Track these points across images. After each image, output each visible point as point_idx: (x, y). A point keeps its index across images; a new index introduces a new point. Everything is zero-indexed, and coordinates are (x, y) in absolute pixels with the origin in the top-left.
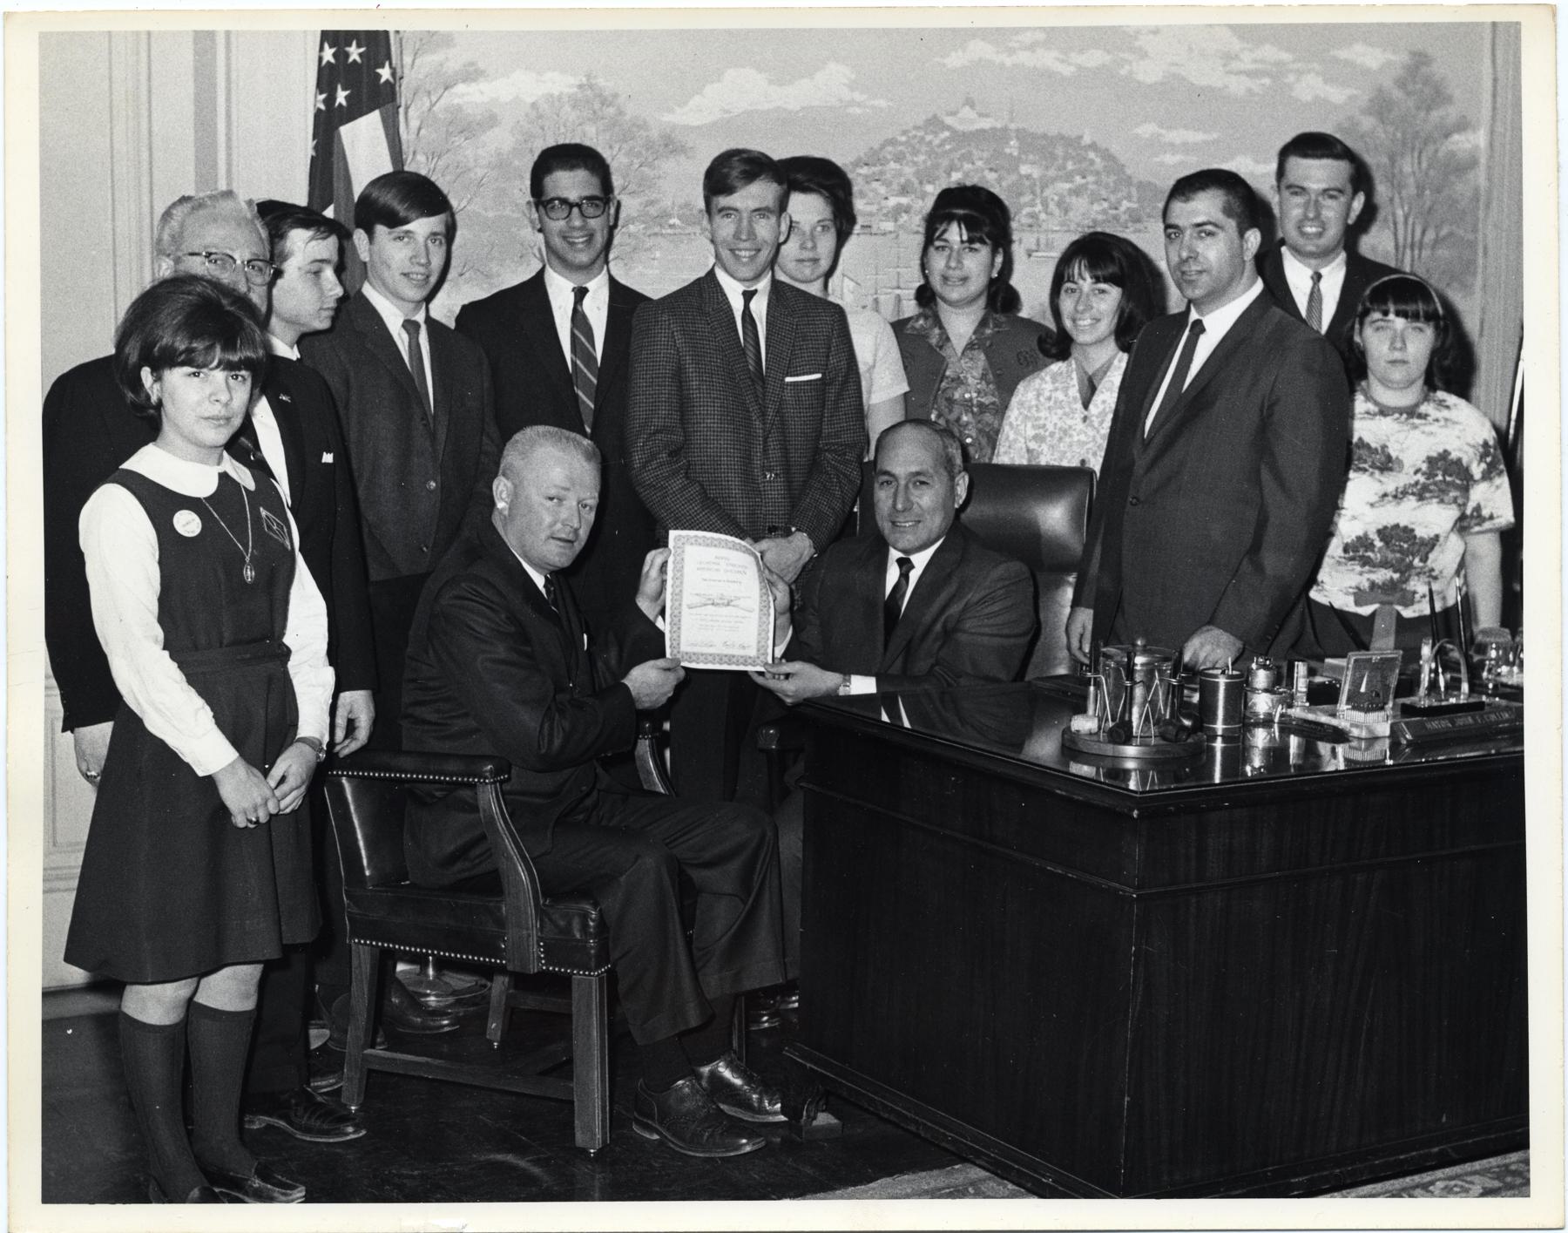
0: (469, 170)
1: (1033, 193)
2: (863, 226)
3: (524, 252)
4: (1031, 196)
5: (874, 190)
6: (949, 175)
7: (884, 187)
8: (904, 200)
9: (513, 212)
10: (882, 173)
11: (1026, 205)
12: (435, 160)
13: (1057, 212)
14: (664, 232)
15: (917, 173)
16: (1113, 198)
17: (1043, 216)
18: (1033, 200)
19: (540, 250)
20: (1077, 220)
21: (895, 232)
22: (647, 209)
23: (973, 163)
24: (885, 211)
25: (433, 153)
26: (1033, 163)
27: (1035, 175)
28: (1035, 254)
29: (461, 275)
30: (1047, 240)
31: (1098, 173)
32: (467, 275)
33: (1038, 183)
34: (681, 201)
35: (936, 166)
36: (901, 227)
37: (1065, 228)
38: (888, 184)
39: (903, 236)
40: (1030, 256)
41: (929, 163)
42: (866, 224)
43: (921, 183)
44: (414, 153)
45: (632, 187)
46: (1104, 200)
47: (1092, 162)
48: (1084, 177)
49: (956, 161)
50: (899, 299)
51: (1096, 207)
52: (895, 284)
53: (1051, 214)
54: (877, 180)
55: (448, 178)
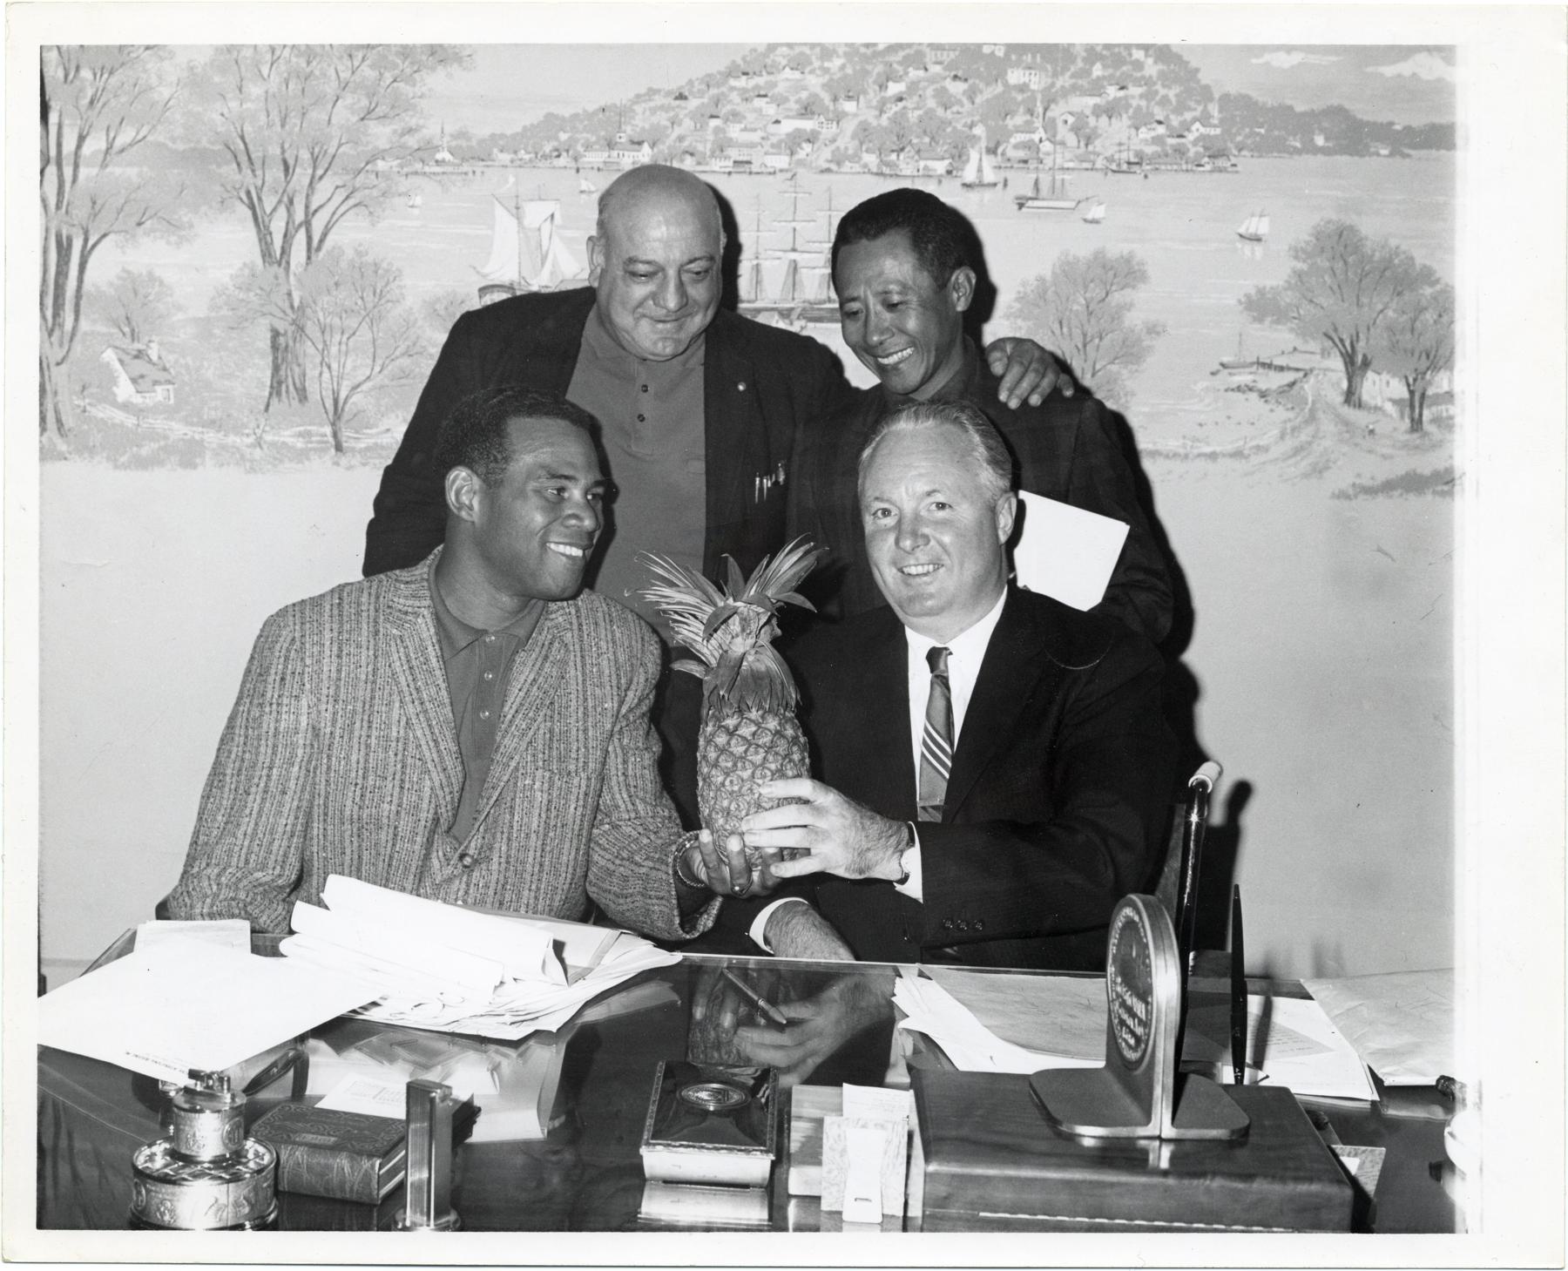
0: (151, 88)
1: (1031, 112)
2: (735, 162)
3: (225, 195)
4: (1028, 117)
5: (759, 111)
6: (882, 87)
7: (774, 106)
8: (807, 125)
9: (213, 144)
10: (774, 85)
11: (1018, 130)
12: (106, 76)
13: (1071, 140)
14: (427, 169)
15: (824, 86)
16: (1175, 121)
17: (1046, 146)
18: (1027, 122)
19: (248, 193)
20: (1108, 154)
21: (787, 171)
22: (403, 140)
23: (926, 69)
24: (774, 140)
25: (103, 68)
26: (1030, 68)
27: (1033, 87)
28: (1030, 203)
29: (139, 224)
30: (1054, 180)
31: (1148, 82)
32: (148, 224)
33: (1039, 97)
34: (448, 129)
35: (866, 73)
36: (801, 163)
37: (1085, 165)
38: (780, 101)
39: (801, 171)
40: (1021, 206)
41: (849, 71)
42: (741, 158)
43: (835, 99)
44: (78, 69)
45: (380, 111)
46: (1160, 122)
47: (1138, 65)
48: (1122, 88)
49: (895, 66)
50: (794, 268)
51: (1144, 133)
52: (790, 246)
53: (1063, 143)
54: (765, 96)
55: (123, 99)
